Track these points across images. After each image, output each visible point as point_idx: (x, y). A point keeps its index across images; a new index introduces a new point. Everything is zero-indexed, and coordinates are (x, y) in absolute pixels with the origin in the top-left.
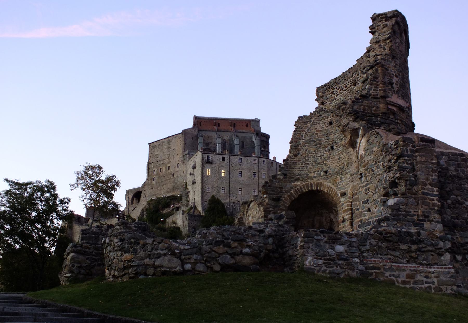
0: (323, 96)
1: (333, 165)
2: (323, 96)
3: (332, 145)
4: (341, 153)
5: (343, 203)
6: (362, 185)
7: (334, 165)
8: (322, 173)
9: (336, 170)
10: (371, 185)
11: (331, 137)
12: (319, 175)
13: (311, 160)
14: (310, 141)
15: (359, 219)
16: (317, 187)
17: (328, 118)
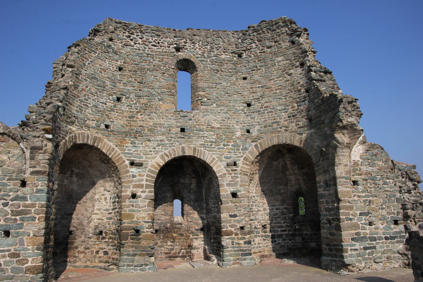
0: (113, 32)
1: (118, 122)
2: (113, 32)
3: (119, 96)
4: (137, 112)
5: (136, 174)
6: (359, 194)
7: (122, 122)
8: (103, 126)
9: (124, 130)
10: (376, 198)
11: (121, 86)
12: (98, 127)
13: (91, 102)
14: (93, 78)
15: (354, 232)
16: (94, 143)
17: (117, 61)
